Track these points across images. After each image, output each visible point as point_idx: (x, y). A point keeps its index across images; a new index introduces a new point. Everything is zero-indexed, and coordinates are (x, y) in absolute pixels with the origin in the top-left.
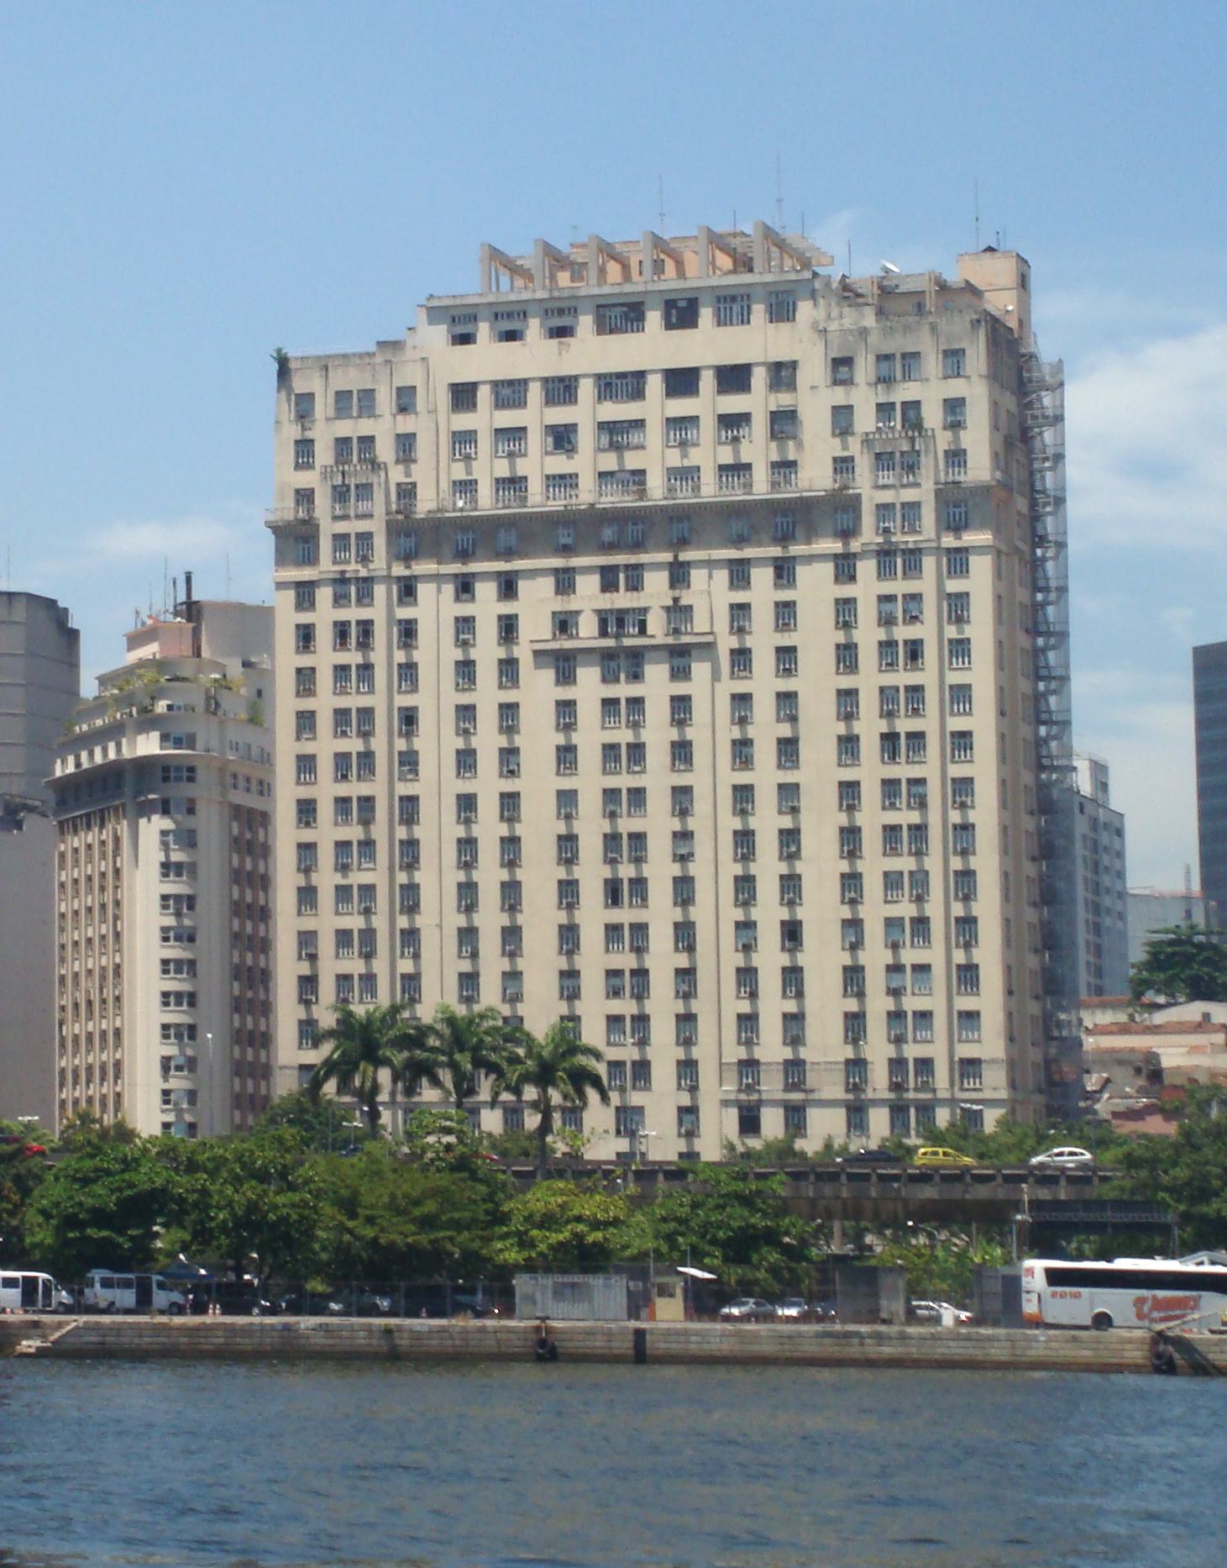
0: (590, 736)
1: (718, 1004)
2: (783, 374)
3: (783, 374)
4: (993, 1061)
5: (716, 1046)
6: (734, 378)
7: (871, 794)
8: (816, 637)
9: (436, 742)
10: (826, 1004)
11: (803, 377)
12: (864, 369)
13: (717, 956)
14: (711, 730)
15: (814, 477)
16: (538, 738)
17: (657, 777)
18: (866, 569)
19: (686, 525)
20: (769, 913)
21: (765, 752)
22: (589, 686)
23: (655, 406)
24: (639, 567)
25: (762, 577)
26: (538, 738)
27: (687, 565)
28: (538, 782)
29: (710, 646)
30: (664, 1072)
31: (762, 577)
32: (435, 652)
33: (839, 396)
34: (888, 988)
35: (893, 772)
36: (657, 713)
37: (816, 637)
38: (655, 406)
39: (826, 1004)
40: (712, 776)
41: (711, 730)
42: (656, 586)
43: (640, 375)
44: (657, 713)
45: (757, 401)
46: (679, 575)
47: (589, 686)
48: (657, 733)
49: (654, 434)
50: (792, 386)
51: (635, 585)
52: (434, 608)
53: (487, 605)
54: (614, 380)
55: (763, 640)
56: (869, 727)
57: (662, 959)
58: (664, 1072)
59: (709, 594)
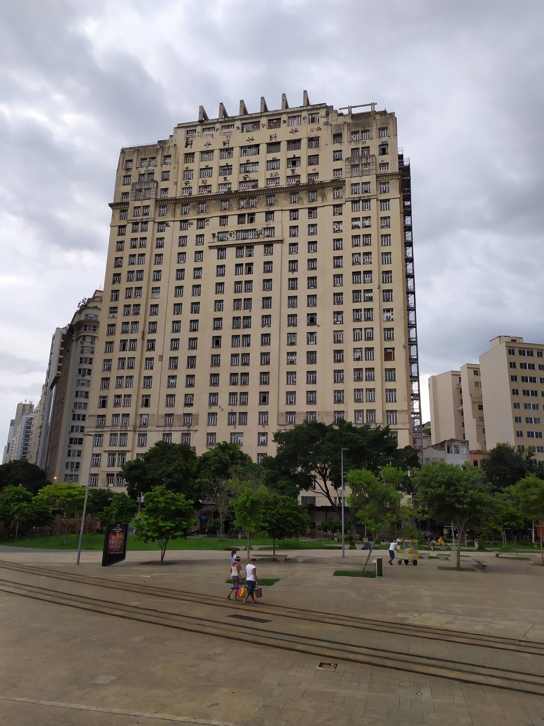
0: (230, 279)
1: (277, 389)
2: (313, 141)
3: (313, 141)
4: (402, 411)
5: (277, 405)
6: (294, 143)
7: (348, 297)
8: (325, 237)
9: (168, 283)
10: (325, 387)
11: (322, 142)
12: (346, 135)
13: (278, 368)
14: (280, 275)
15: (325, 174)
16: (209, 279)
17: (257, 294)
18: (347, 207)
19: (273, 198)
20: (302, 347)
21: (302, 283)
22: (231, 258)
23: (263, 156)
24: (254, 214)
25: (303, 214)
26: (209, 279)
27: (273, 212)
28: (208, 297)
29: (281, 241)
30: (253, 418)
31: (303, 214)
32: (171, 249)
33: (337, 147)
34: (354, 359)
35: (357, 287)
36: (258, 268)
37: (325, 237)
38: (263, 156)
39: (325, 387)
40: (280, 292)
41: (280, 275)
42: (260, 221)
43: (257, 146)
44: (258, 268)
45: (303, 152)
46: (269, 214)
47: (231, 258)
48: (258, 276)
49: (262, 166)
50: (317, 146)
51: (252, 220)
52: (172, 233)
53: (192, 232)
54: (247, 149)
55: (303, 239)
56: (347, 269)
57: (255, 368)
58: (253, 418)
59: (281, 222)
